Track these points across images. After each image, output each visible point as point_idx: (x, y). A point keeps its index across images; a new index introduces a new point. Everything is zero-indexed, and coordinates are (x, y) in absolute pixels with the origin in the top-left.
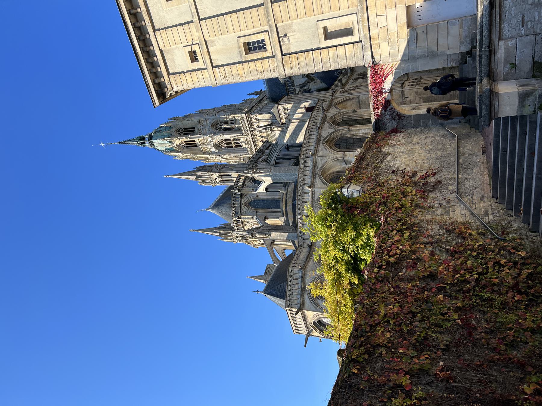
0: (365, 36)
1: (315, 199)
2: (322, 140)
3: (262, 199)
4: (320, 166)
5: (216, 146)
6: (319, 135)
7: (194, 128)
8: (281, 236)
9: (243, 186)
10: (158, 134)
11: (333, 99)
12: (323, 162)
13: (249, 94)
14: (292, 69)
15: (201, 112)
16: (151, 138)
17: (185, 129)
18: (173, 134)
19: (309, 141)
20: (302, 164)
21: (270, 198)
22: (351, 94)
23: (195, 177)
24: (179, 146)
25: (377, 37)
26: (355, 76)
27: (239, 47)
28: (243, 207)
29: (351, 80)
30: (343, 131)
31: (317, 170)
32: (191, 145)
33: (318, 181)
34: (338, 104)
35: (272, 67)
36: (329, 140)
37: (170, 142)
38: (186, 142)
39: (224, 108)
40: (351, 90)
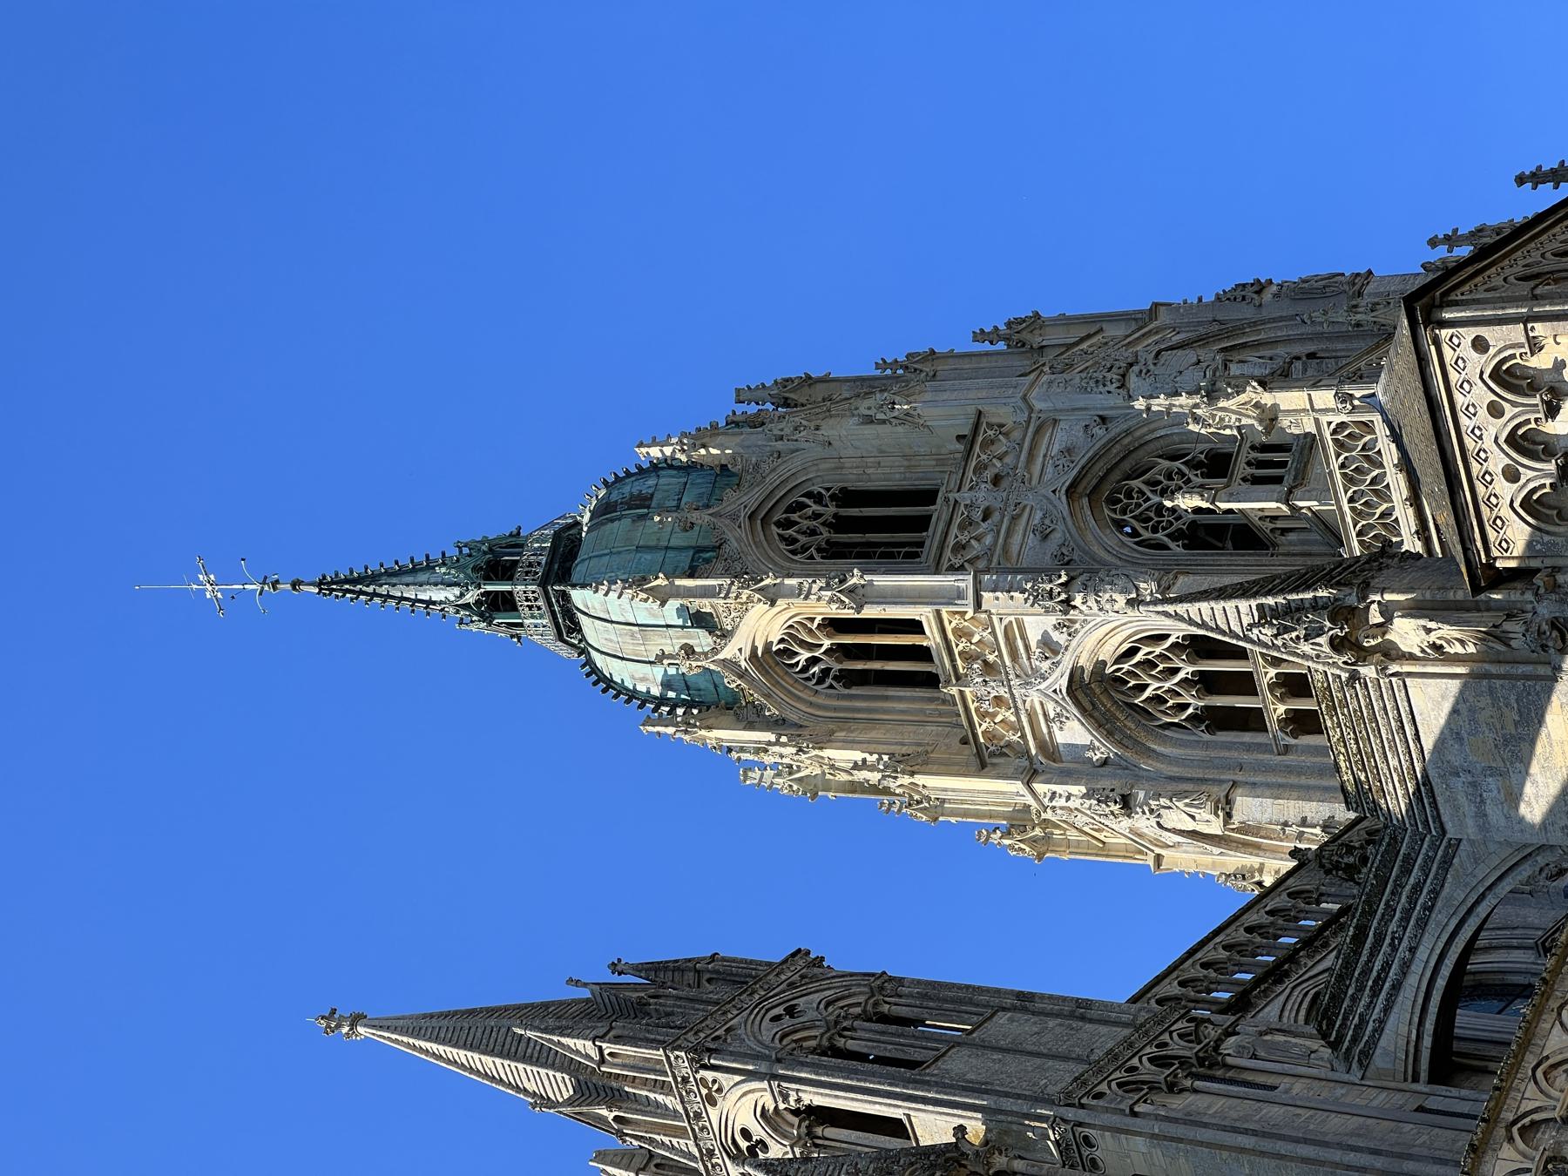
5: (1096, 692)
7: (929, 496)
10: (619, 528)
15: (1024, 341)
16: (564, 560)
17: (847, 497)
18: (737, 538)
23: (560, 1086)
24: (772, 659)
32: (878, 670)
37: (701, 620)
39: (1246, 312)
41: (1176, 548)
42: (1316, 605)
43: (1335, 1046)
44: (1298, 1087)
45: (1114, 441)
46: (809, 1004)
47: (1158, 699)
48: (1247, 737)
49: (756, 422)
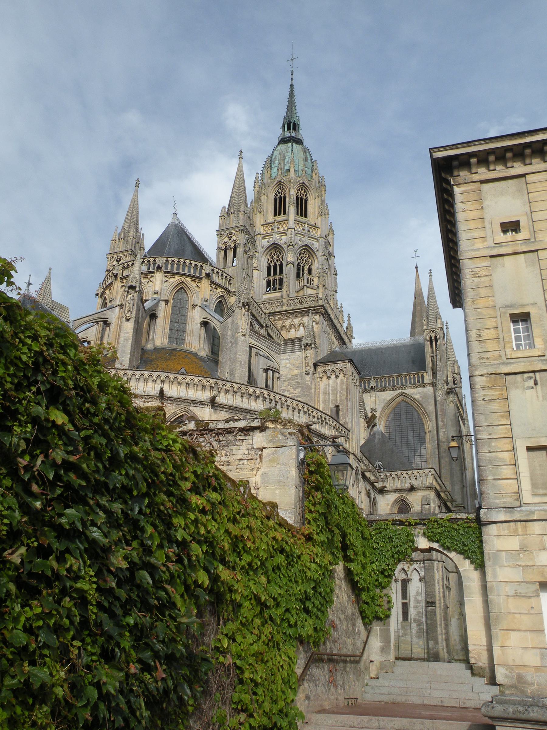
0: (532, 513)
1: (191, 408)
3: (190, 314)
7: (306, 217)
8: (126, 339)
9: (212, 282)
13: (349, 317)
14: (483, 388)
17: (306, 201)
19: (291, 408)
21: (189, 328)
25: (528, 533)
27: (523, 306)
29: (368, 487)
35: (488, 355)
38: (285, 198)
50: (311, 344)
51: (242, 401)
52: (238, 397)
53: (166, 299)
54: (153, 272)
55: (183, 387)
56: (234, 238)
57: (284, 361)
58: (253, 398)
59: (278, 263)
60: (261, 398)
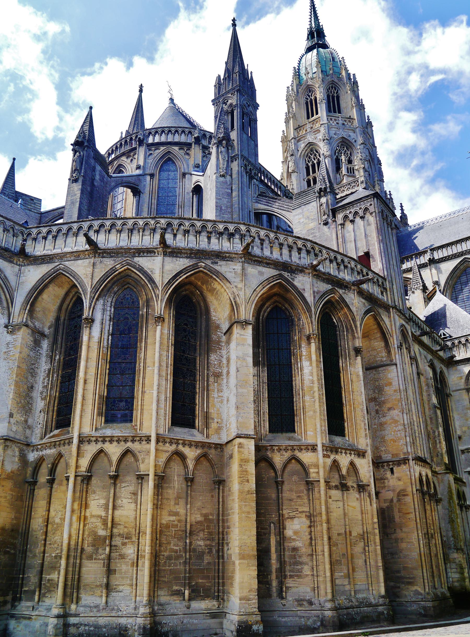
1: (136, 259)
2: (286, 274)
3: (179, 184)
4: (217, 267)
6: (300, 270)
7: (340, 112)
11: (387, 308)
12: (228, 275)
13: (402, 206)
17: (338, 97)
20: (226, 229)
21: (179, 200)
22: (400, 347)
26: (439, 366)
28: (162, 148)
29: (430, 357)
30: (308, 324)
31: (209, 262)
33: (182, 263)
34: (376, 319)
36: (287, 290)
39: (376, 162)
40: (409, 349)
41: (335, 157)
42: (326, 185)
43: (257, 197)
44: (250, 192)
45: (352, 144)
46: (251, 109)
47: (310, 158)
48: (305, 174)
49: (350, 79)
50: (325, 189)
51: (209, 243)
52: (203, 238)
53: (150, 172)
54: (135, 149)
55: (124, 235)
56: (230, 101)
57: (297, 217)
58: (225, 237)
59: (315, 162)
60: (237, 236)
